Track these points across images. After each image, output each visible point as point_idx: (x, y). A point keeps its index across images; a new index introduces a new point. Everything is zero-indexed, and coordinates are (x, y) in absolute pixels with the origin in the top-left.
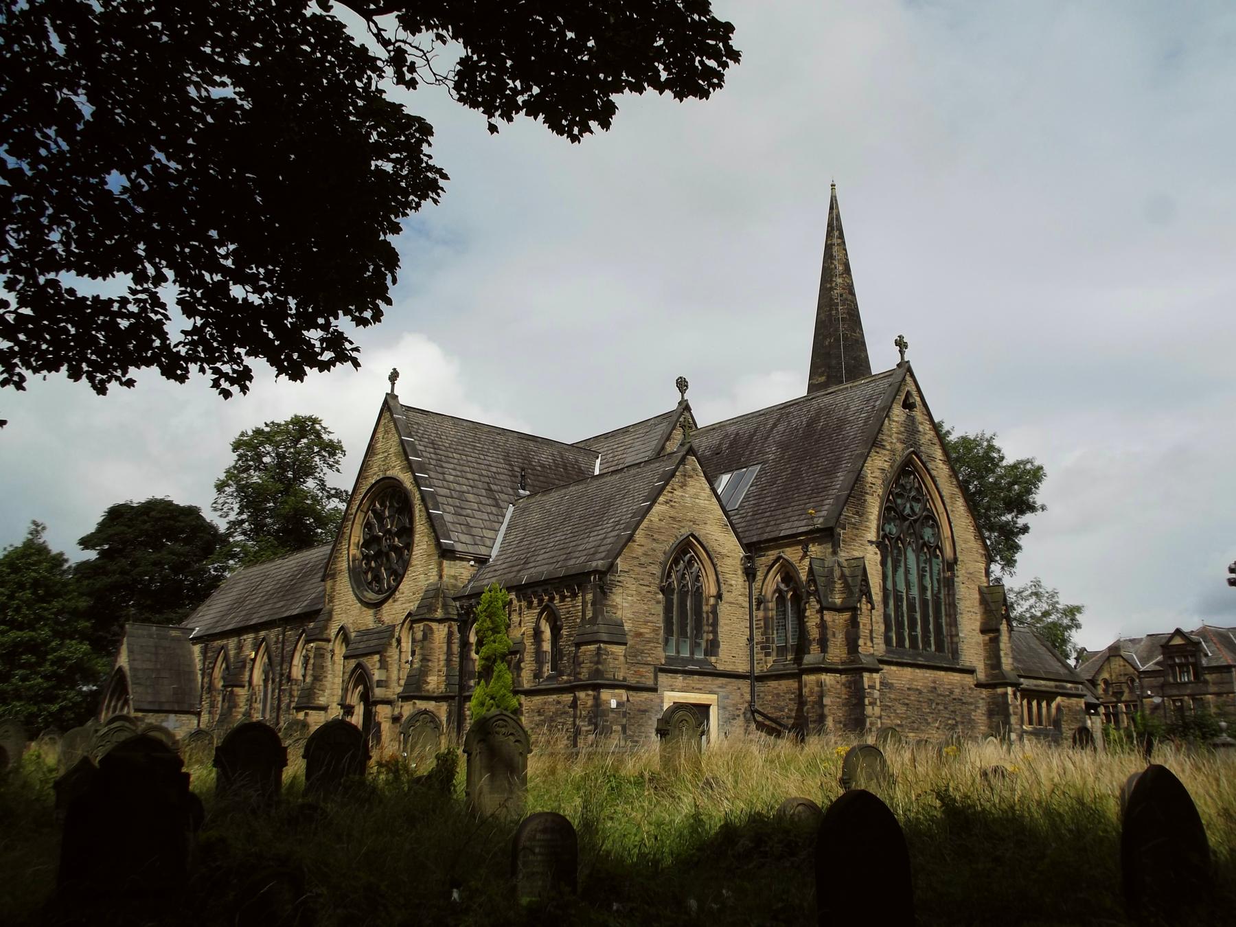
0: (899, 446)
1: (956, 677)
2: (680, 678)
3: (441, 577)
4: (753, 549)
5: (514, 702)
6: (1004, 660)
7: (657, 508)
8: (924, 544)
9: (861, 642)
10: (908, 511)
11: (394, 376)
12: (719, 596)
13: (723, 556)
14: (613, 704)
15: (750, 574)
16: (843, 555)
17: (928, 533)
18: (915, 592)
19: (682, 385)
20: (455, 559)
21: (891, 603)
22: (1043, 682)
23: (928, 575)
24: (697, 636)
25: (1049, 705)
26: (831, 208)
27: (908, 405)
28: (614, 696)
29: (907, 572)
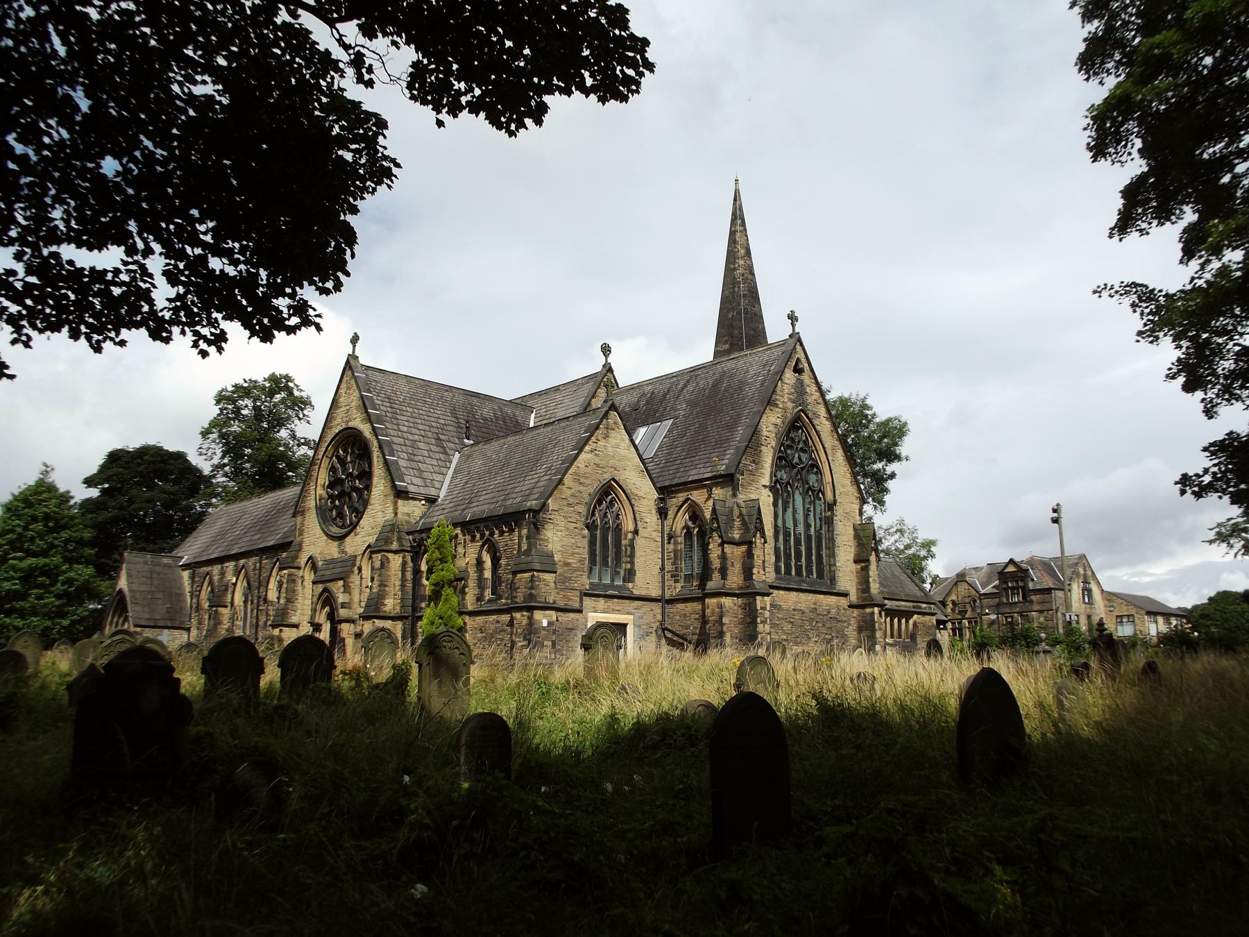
0: (790, 405)
1: (834, 599)
2: (602, 600)
3: (396, 514)
4: (665, 492)
5: (460, 621)
6: (872, 585)
7: (583, 456)
8: (810, 488)
9: (755, 571)
10: (796, 460)
11: (355, 340)
12: (636, 532)
13: (640, 498)
14: (545, 623)
15: (662, 513)
16: (741, 497)
17: (812, 479)
18: (801, 529)
19: (606, 350)
20: (408, 498)
21: (781, 538)
24: (616, 566)
25: (907, 622)
26: (735, 200)
27: (798, 370)
28: (545, 616)
29: (795, 511)
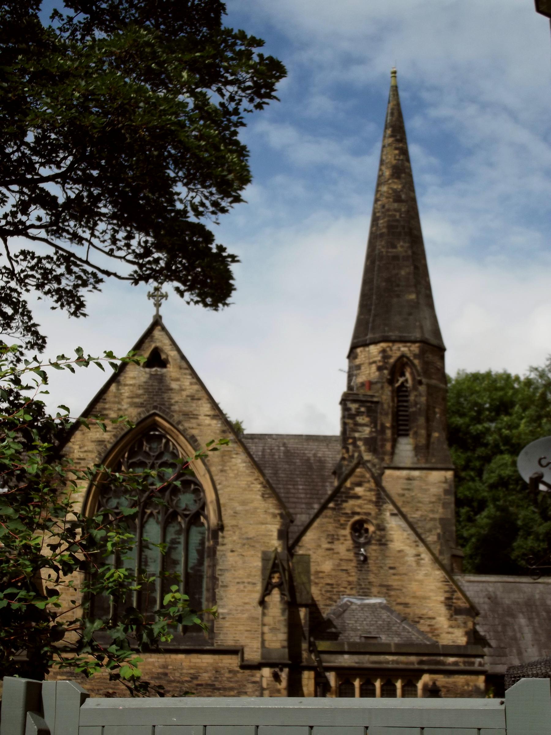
1: (207, 659)
22: (390, 658)
23: (181, 548)
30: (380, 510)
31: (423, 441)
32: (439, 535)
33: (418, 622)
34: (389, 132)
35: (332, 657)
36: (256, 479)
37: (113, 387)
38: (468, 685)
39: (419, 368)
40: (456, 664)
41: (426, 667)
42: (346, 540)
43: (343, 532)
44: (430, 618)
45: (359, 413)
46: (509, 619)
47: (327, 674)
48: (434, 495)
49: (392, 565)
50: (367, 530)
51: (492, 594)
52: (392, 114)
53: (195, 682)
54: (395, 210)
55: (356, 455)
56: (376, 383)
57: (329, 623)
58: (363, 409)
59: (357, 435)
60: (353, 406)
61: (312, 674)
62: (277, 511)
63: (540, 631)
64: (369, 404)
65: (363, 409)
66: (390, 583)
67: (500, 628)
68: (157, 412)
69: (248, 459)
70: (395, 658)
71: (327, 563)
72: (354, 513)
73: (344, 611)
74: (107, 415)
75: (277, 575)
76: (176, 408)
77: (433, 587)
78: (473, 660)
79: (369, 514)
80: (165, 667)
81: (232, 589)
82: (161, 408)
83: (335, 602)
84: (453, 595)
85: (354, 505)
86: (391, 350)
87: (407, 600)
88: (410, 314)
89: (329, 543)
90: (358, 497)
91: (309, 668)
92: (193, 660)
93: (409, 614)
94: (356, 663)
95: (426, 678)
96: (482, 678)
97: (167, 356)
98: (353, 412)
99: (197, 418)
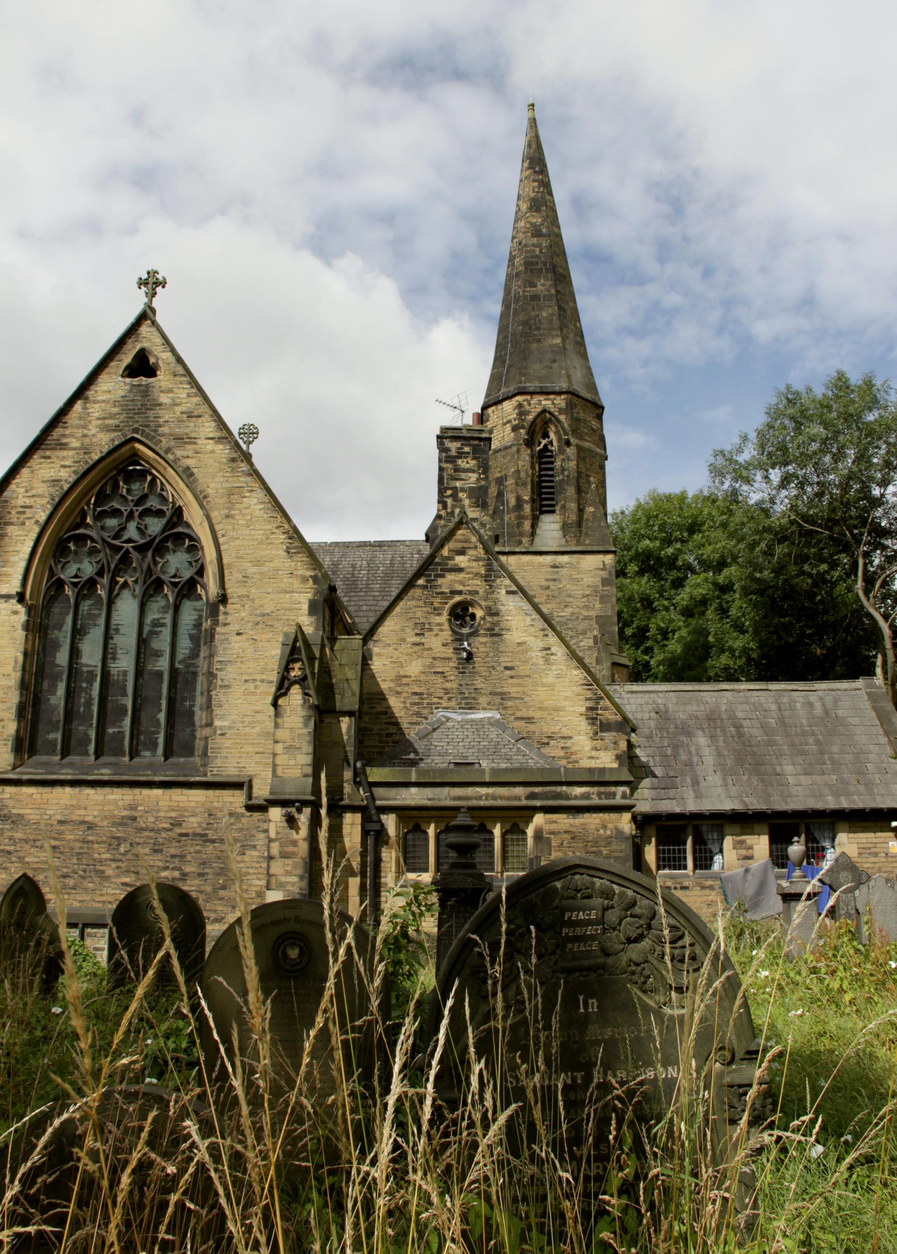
1: (197, 796)
18: (125, 663)
22: (483, 791)
23: (166, 632)
30: (491, 587)
31: (574, 517)
32: (595, 637)
33: (548, 744)
34: (526, 165)
35: (392, 792)
36: (278, 527)
37: (78, 406)
38: (605, 827)
39: (566, 425)
40: (586, 796)
41: (538, 803)
42: (441, 630)
43: (438, 619)
44: (564, 738)
45: (461, 455)
46: (683, 739)
47: (383, 817)
48: (588, 586)
49: (509, 665)
50: (473, 617)
51: (662, 707)
52: (529, 146)
53: (178, 830)
54: (534, 245)
55: (457, 511)
56: (511, 446)
57: (409, 747)
58: (467, 449)
59: (458, 484)
60: (453, 446)
61: (358, 817)
62: (309, 573)
63: (726, 753)
64: (476, 442)
65: (467, 449)
66: (506, 690)
67: (669, 752)
68: (138, 436)
69: (267, 499)
70: (490, 790)
71: (414, 663)
72: (454, 593)
73: (434, 730)
74: (65, 444)
75: (298, 665)
76: (165, 430)
77: (568, 694)
78: (613, 789)
79: (477, 592)
80: (133, 807)
81: (237, 691)
82: (143, 431)
83: (426, 718)
84: (597, 703)
85: (455, 581)
86: (529, 404)
87: (531, 714)
88: (554, 361)
89: (417, 634)
90: (461, 570)
91: (353, 809)
92: (175, 798)
93: (534, 732)
94: (430, 799)
95: (539, 819)
96: (627, 816)
97: (158, 359)
98: (453, 453)
99: (196, 443)
